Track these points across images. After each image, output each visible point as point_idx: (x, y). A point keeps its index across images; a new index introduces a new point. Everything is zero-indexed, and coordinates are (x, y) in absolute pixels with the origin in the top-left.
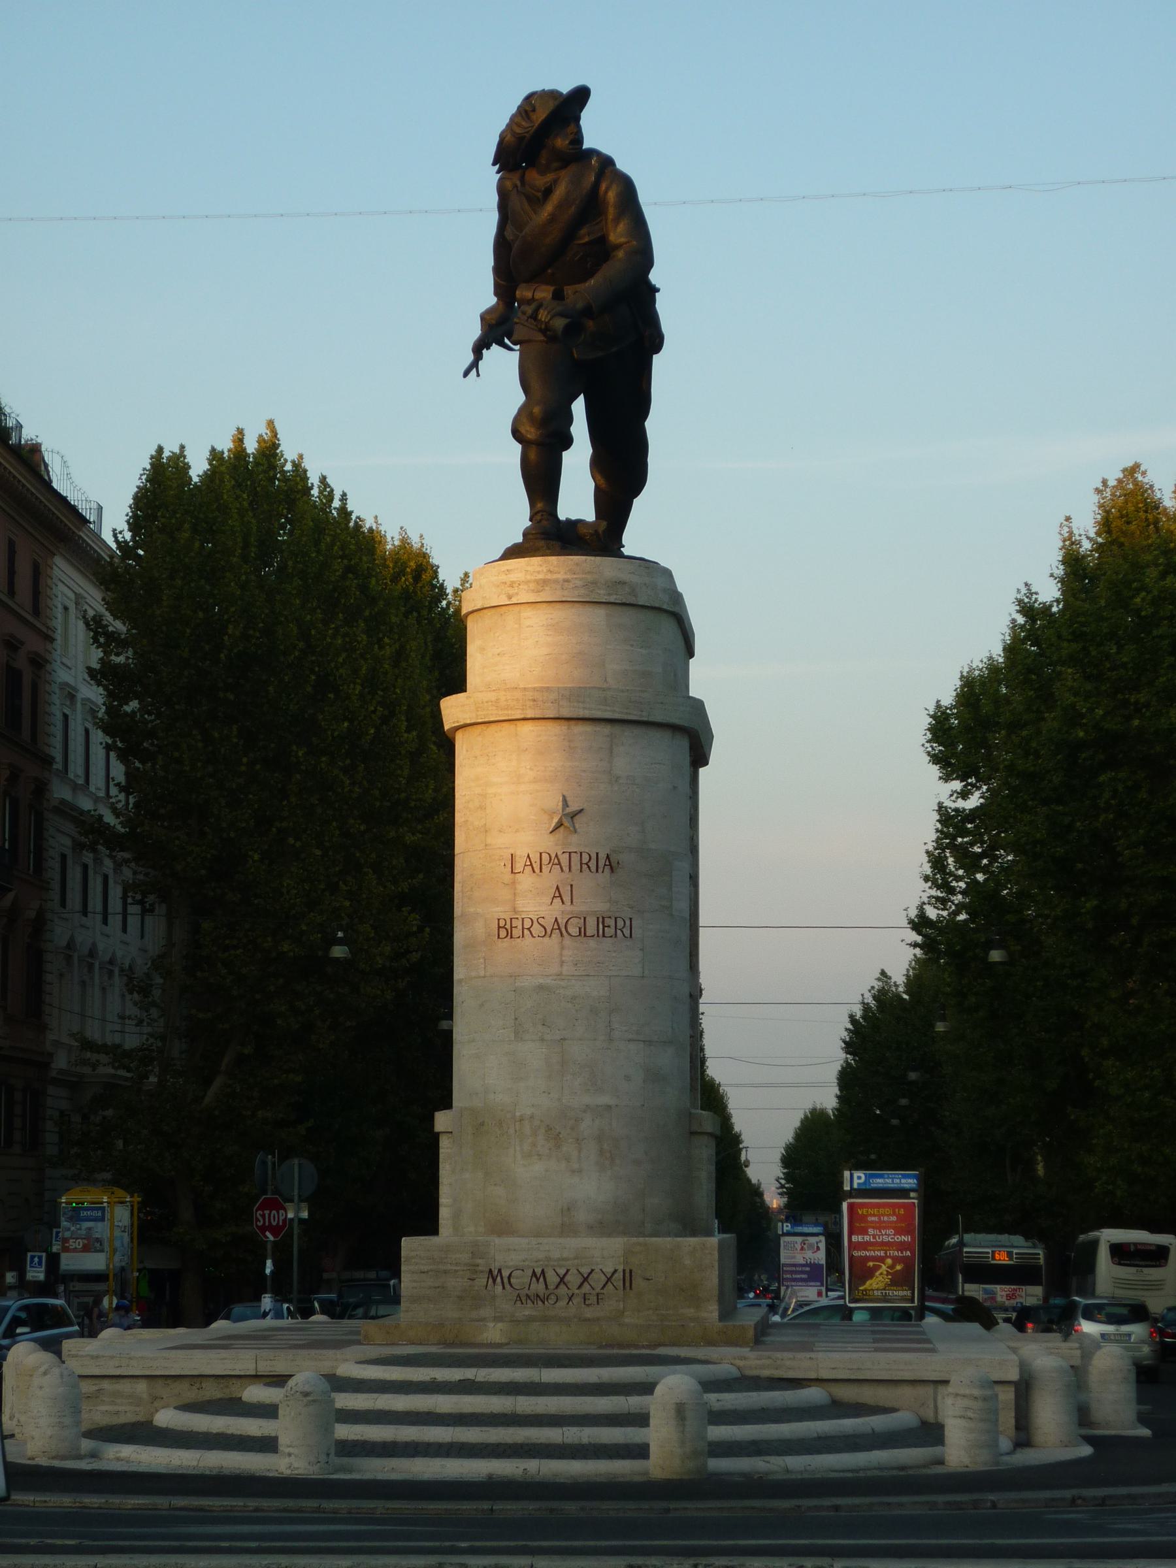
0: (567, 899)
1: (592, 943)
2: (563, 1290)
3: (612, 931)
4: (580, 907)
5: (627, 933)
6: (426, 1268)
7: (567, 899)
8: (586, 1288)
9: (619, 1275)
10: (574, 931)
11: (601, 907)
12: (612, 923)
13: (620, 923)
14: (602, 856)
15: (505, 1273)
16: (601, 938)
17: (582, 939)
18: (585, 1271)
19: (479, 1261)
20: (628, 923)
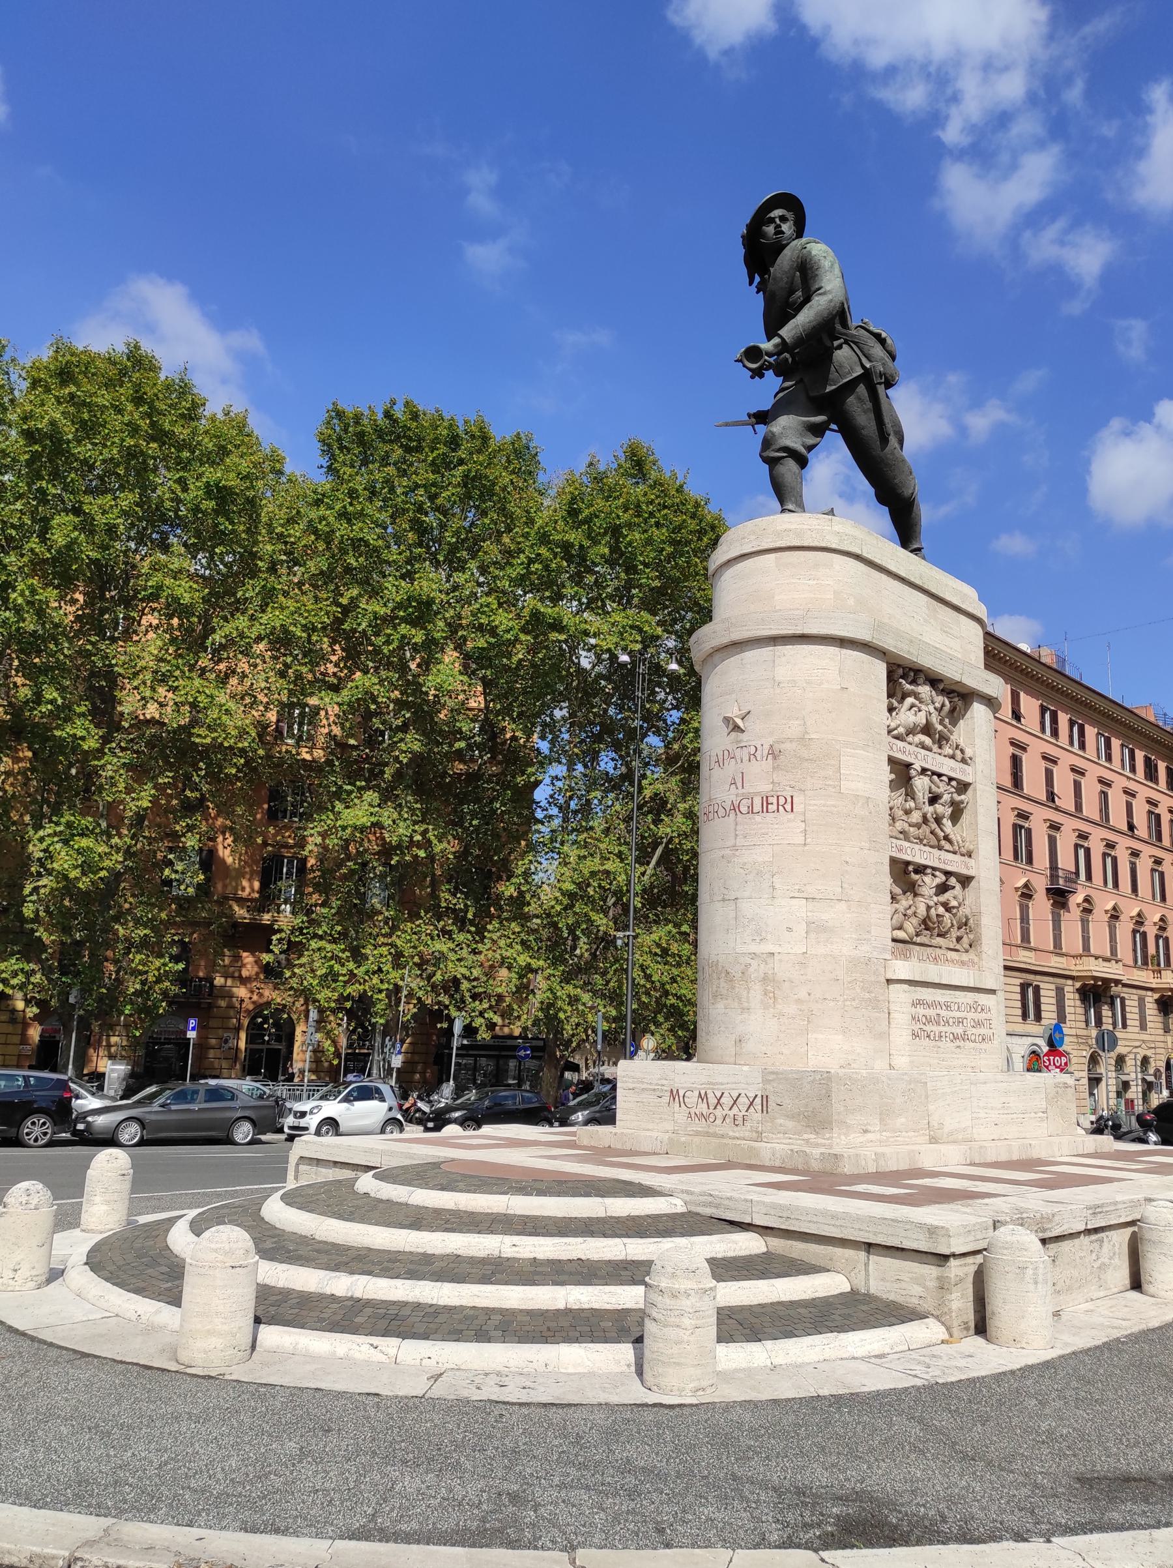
0: (739, 785)
1: (758, 818)
2: (719, 1112)
3: (774, 807)
4: (748, 789)
5: (788, 807)
6: (631, 1086)
7: (739, 785)
8: (735, 1110)
9: (758, 1100)
10: (744, 809)
11: (765, 788)
12: (775, 801)
13: (782, 800)
14: (766, 747)
15: (681, 1094)
16: (765, 814)
17: (750, 815)
18: (735, 1095)
19: (664, 1082)
20: (789, 800)
